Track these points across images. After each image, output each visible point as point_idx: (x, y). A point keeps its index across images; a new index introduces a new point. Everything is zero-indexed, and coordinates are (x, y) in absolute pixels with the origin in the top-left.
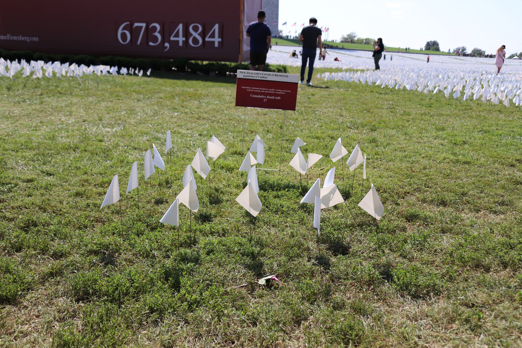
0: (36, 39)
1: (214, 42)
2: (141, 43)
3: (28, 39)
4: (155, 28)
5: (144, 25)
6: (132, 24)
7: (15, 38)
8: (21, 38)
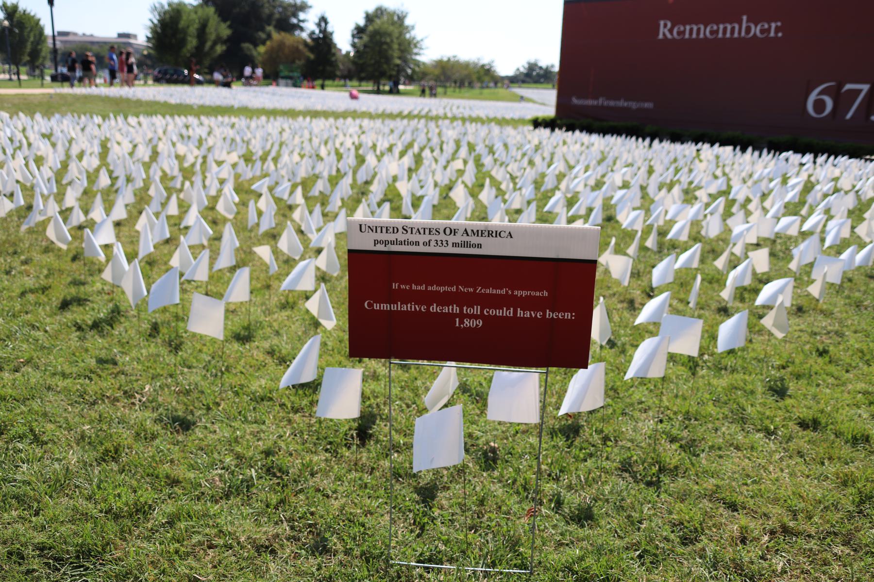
0: (648, 105)
2: (852, 117)
3: (634, 105)
5: (865, 88)
6: (840, 86)
7: (612, 103)
8: (622, 103)
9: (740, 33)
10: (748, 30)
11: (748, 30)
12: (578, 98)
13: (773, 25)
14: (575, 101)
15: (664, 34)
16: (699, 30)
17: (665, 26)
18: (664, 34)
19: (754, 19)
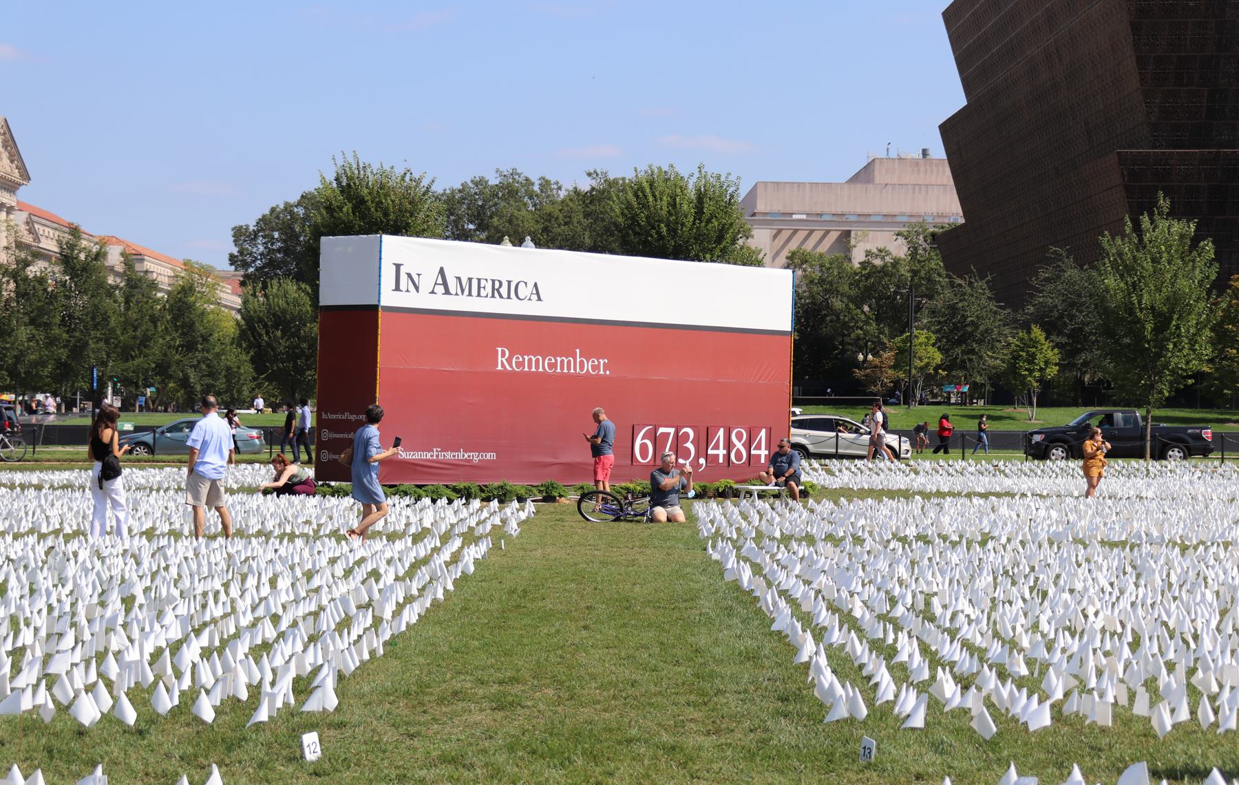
0: (490, 456)
1: (759, 456)
3: (475, 457)
4: (687, 434)
5: (672, 431)
7: (449, 456)
8: (462, 455)
10: (582, 363)
11: (582, 368)
16: (537, 361)
17: (503, 354)
19: (587, 355)
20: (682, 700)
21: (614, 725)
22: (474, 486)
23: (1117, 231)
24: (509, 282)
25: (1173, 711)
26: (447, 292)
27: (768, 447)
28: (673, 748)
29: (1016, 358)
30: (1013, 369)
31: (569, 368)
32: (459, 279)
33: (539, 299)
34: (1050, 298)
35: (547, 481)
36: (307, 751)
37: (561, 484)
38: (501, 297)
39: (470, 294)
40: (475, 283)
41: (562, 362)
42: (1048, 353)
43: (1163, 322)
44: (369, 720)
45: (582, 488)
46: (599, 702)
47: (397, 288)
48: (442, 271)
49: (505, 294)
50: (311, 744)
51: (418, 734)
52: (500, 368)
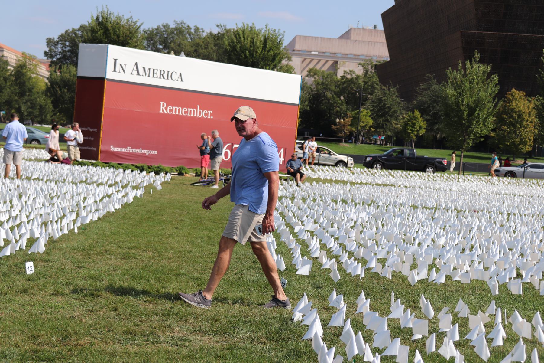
0: (155, 152)
3: (147, 152)
6: (232, 145)
7: (135, 151)
8: (140, 151)
9: (197, 115)
10: (200, 112)
11: (200, 114)
12: (114, 147)
13: (209, 112)
14: (113, 149)
15: (163, 110)
16: (179, 109)
18: (163, 110)
19: (202, 108)
20: (209, 260)
21: (174, 268)
22: (145, 166)
23: (455, 67)
24: (168, 72)
25: (418, 273)
26: (138, 74)
27: (284, 157)
28: (197, 279)
29: (406, 124)
30: (405, 130)
31: (194, 114)
32: (144, 68)
33: (182, 81)
34: (424, 98)
35: (181, 166)
36: (27, 270)
37: (186, 167)
38: (164, 78)
39: (149, 76)
40: (152, 71)
41: (191, 111)
42: (421, 124)
43: (472, 111)
44: (61, 259)
45: (196, 170)
46: (170, 259)
47: (115, 71)
48: (136, 64)
49: (166, 77)
50: (30, 267)
51: (83, 267)
52: (161, 111)
